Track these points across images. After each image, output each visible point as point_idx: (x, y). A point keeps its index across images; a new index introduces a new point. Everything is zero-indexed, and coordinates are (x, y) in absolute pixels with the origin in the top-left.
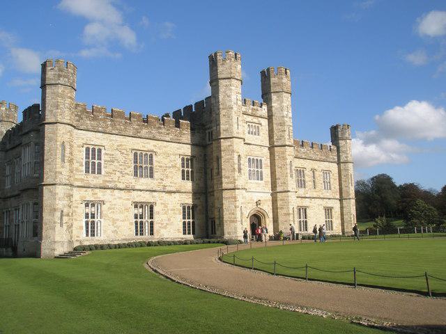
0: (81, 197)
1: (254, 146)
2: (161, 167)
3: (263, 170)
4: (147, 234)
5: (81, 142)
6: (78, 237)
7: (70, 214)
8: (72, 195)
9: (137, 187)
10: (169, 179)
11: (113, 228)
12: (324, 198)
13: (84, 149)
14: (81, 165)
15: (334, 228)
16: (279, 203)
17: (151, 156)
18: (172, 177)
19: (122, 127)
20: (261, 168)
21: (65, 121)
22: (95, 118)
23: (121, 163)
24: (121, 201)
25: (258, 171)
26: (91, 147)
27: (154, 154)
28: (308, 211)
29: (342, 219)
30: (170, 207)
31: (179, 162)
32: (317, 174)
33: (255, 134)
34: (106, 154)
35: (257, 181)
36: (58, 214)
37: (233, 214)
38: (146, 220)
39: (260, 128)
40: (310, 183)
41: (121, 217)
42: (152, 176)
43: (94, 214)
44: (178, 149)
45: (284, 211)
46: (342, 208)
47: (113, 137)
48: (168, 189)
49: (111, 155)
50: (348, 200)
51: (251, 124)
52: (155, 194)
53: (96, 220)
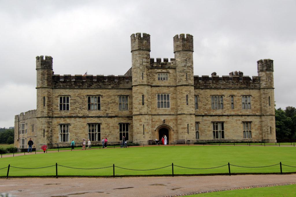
0: (57, 123)
1: (163, 87)
2: (104, 103)
3: (170, 101)
4: (96, 140)
5: (57, 95)
6: (56, 142)
7: (49, 131)
8: (51, 122)
9: (90, 115)
10: (111, 110)
11: (75, 137)
12: (242, 116)
13: (59, 98)
14: (58, 106)
15: (253, 135)
16: (179, 121)
17: (99, 98)
18: (112, 109)
19: (81, 84)
20: (168, 99)
21: (45, 86)
22: (64, 82)
23: (80, 103)
24: (80, 123)
25: (165, 102)
26: (63, 97)
27: (101, 97)
28: (225, 125)
29: (261, 130)
30: (111, 125)
31: (117, 99)
32: (235, 99)
33: (164, 79)
34: (72, 99)
35: (165, 108)
36: (43, 131)
37: (138, 129)
38: (97, 132)
39: (168, 75)
40: (229, 105)
41: (81, 131)
42: (99, 108)
43: (65, 131)
44: (117, 92)
45: (182, 126)
46: (262, 121)
47: (75, 90)
48: (110, 115)
49: (74, 100)
50: (266, 117)
51: (160, 74)
52: (101, 118)
53: (66, 133)
